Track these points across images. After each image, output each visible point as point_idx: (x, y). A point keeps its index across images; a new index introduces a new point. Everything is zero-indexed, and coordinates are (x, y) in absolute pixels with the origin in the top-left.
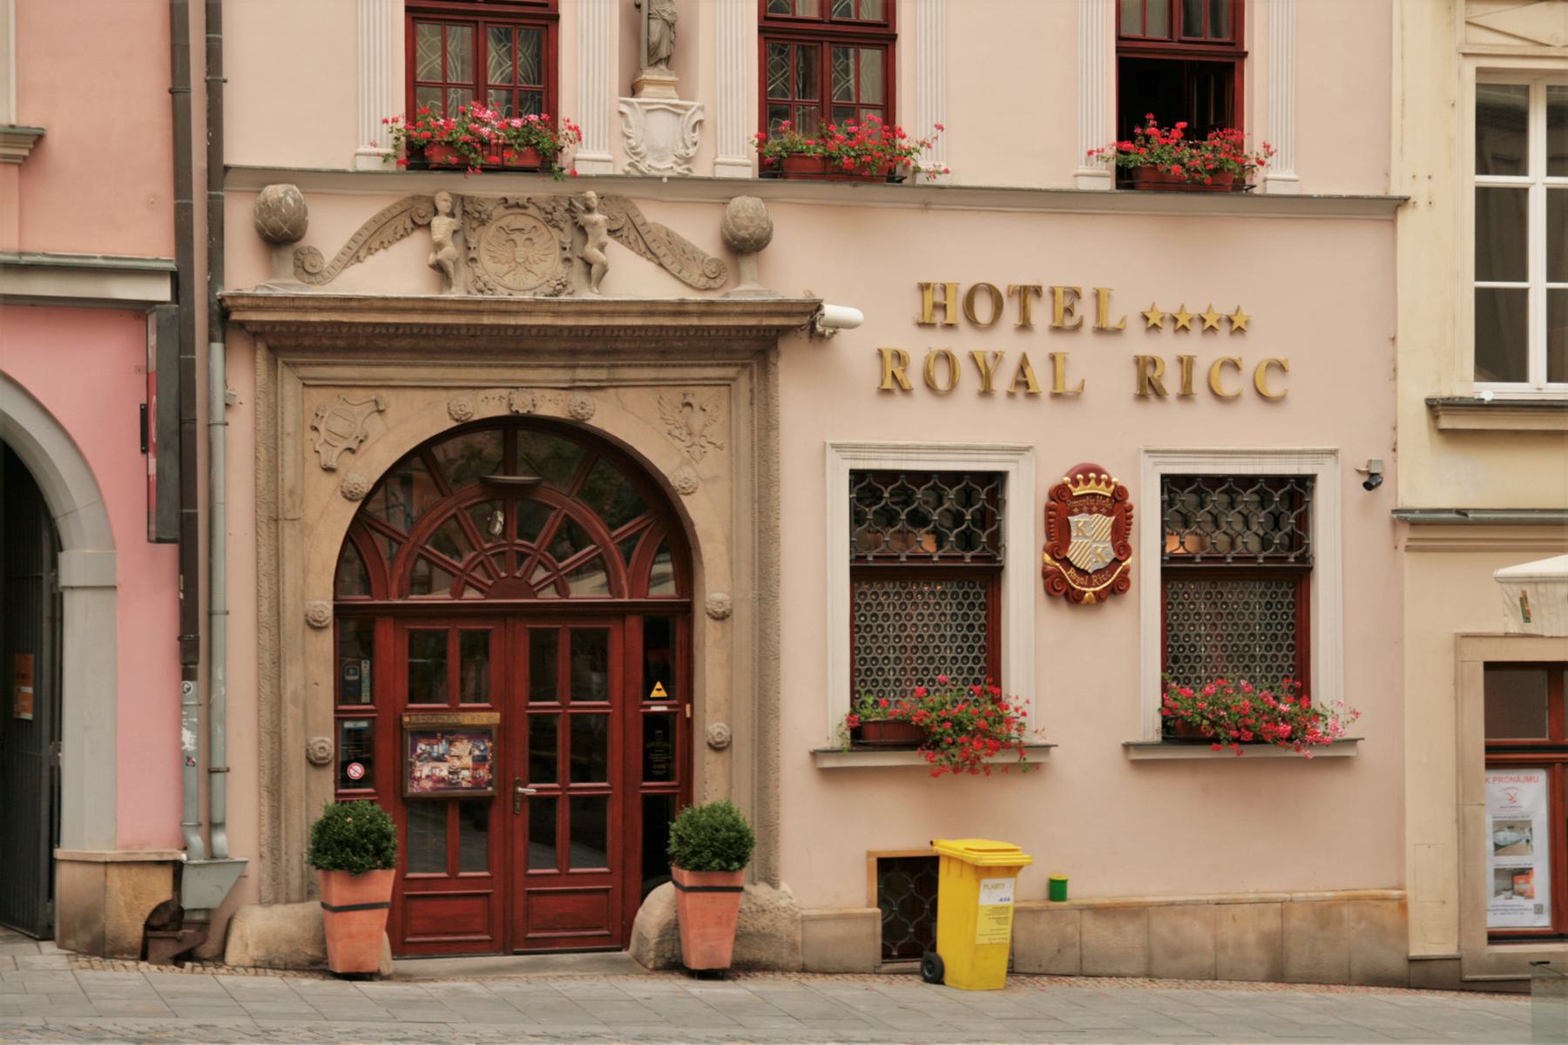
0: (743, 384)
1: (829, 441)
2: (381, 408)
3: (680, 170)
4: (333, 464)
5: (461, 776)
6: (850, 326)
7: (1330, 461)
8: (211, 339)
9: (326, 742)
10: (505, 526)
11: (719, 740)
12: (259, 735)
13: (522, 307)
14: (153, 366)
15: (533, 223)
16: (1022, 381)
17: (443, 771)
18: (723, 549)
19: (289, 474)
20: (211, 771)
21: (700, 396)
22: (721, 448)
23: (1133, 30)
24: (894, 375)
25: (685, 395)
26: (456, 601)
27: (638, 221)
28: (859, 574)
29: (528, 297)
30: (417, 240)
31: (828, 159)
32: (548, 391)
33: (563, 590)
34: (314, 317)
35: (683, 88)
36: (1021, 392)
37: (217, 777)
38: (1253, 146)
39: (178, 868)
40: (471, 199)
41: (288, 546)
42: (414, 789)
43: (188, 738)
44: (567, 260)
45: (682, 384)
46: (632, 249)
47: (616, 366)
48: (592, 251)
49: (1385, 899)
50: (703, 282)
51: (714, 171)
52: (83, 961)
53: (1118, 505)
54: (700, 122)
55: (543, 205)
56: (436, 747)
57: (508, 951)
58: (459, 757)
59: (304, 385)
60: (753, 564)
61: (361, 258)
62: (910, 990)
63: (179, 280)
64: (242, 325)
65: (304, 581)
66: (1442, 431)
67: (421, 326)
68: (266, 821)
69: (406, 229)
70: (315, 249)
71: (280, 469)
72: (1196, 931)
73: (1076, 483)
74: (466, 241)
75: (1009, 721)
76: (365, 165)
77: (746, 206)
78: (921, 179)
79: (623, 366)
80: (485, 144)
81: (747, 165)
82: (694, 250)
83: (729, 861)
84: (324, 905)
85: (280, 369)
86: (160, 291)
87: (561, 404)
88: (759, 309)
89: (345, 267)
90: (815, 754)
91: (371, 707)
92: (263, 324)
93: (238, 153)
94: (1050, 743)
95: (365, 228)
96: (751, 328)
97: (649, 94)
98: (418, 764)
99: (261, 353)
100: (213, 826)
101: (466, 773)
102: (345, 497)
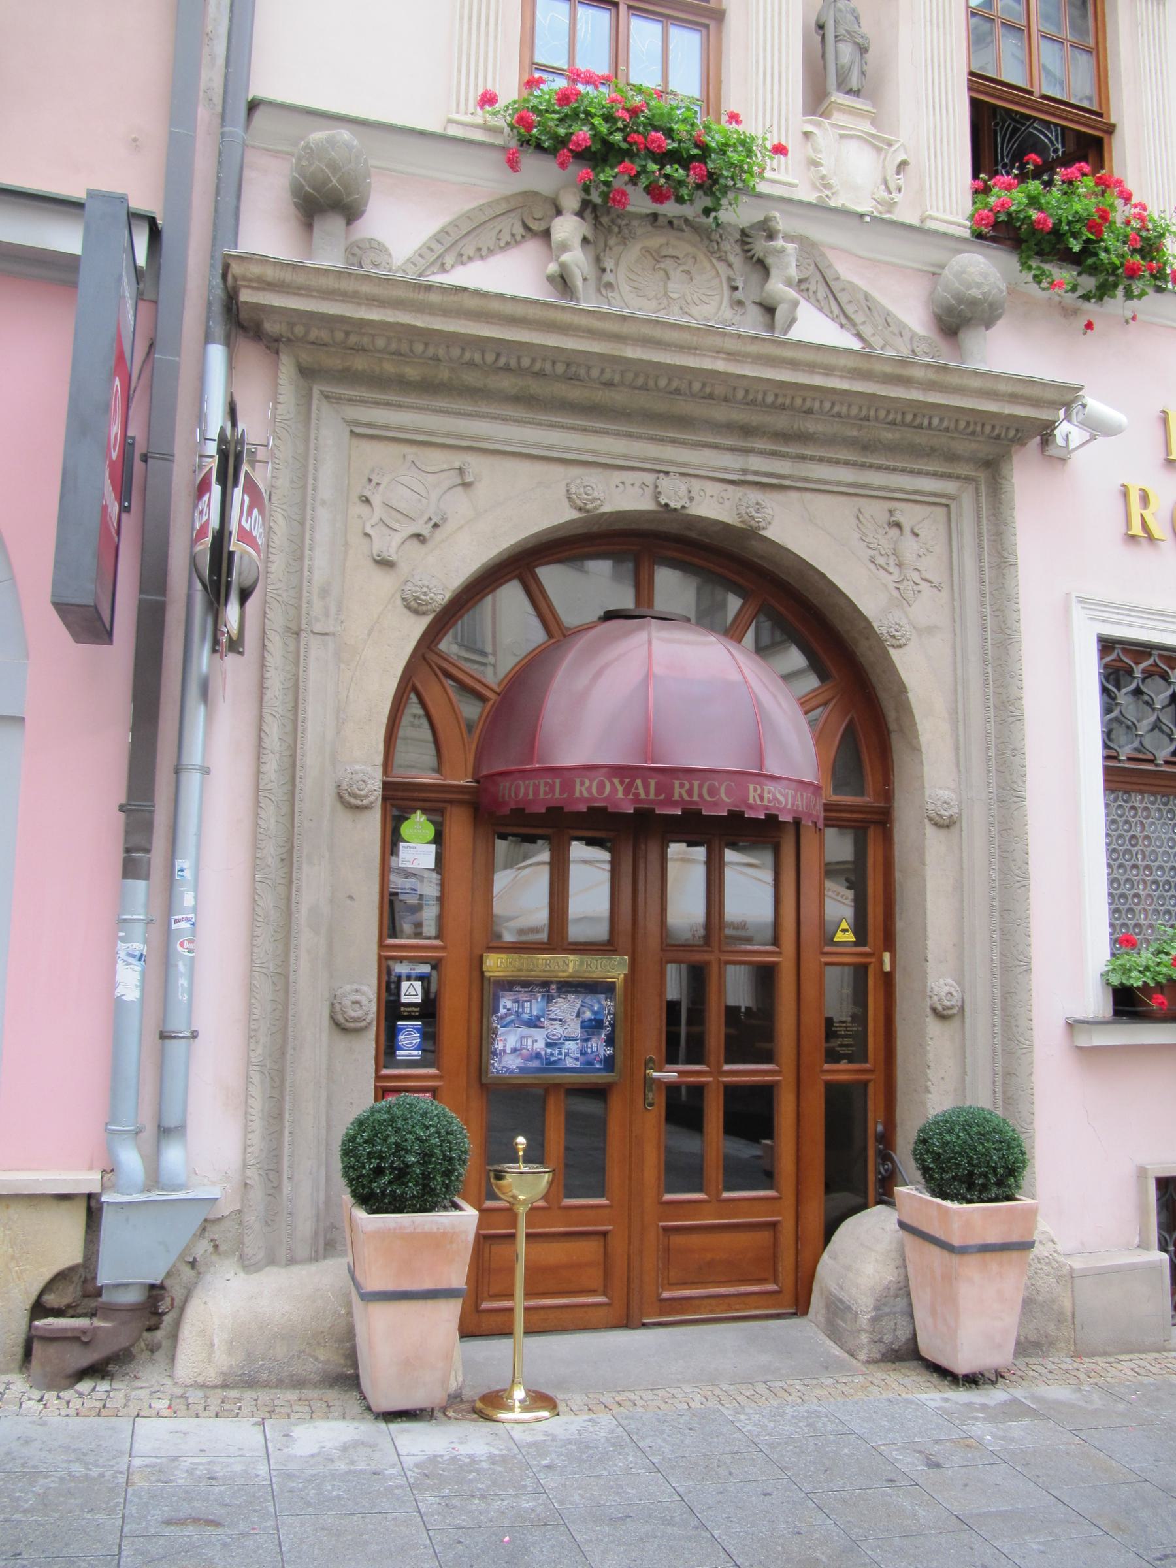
2: (469, 479)
4: (391, 554)
5: (563, 1051)
8: (208, 339)
9: (363, 994)
17: (537, 1041)
19: (320, 562)
20: (164, 1036)
21: (908, 515)
22: (938, 588)
25: (891, 512)
27: (829, 276)
32: (709, 484)
34: (374, 315)
41: (314, 676)
44: (740, 303)
45: (885, 495)
46: (821, 309)
54: (903, 164)
56: (527, 1005)
59: (352, 431)
61: (448, 266)
69: (513, 235)
70: (379, 243)
71: (307, 552)
79: (812, 458)
81: (964, 226)
85: (315, 402)
87: (727, 503)
90: (1073, 1026)
98: (501, 1030)
100: (166, 1132)
102: (408, 607)
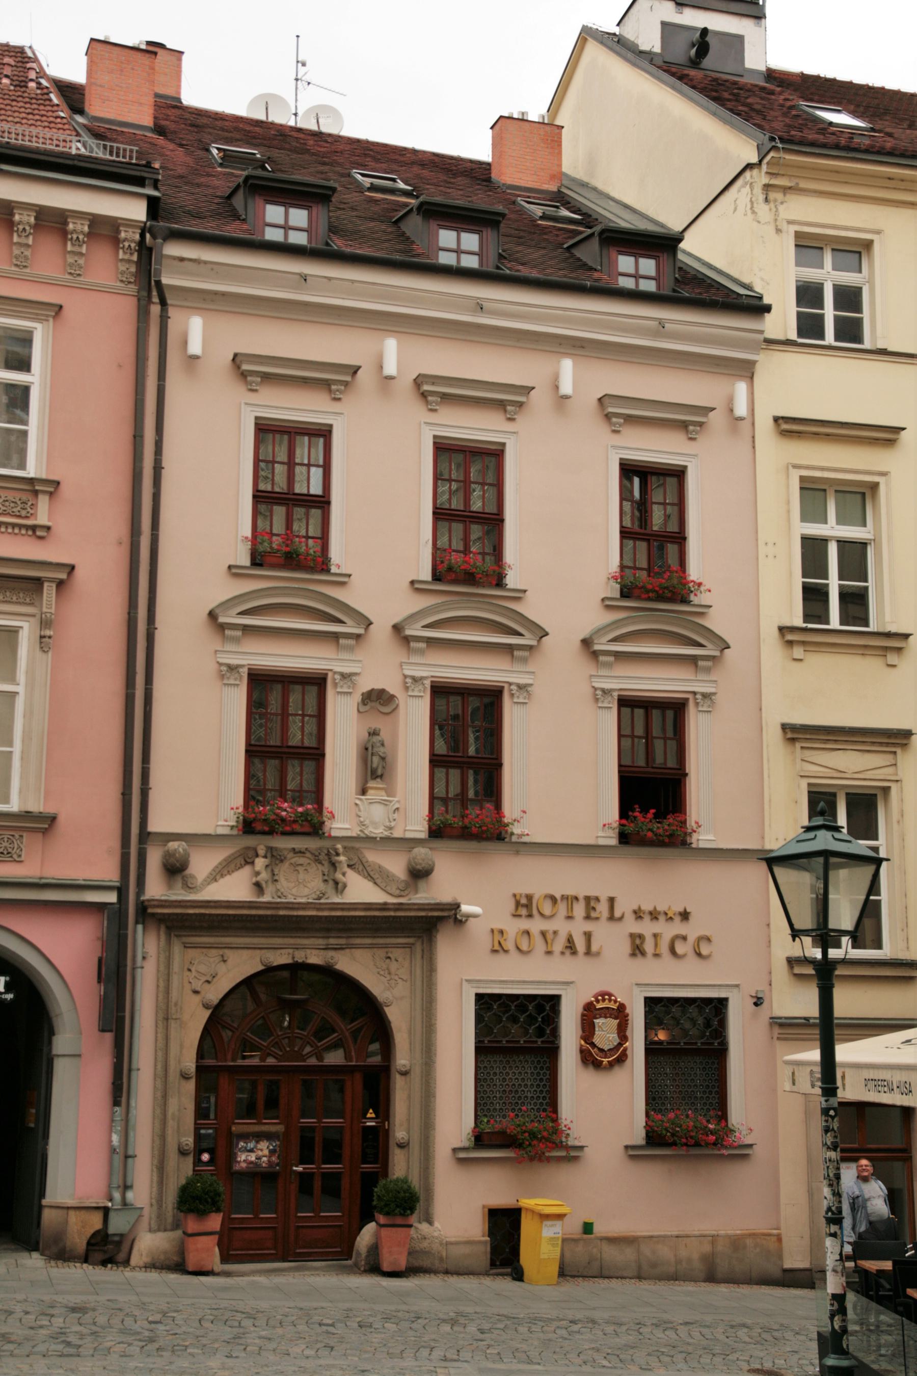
0: (418, 947)
1: (465, 978)
2: (225, 959)
3: (387, 833)
4: (198, 989)
6: (476, 916)
7: (735, 990)
8: (137, 922)
10: (290, 1022)
11: (402, 1141)
12: (153, 1136)
13: (300, 906)
14: (105, 939)
15: (308, 861)
16: (570, 946)
17: (252, 1157)
18: (406, 1036)
19: (174, 994)
21: (396, 953)
22: (406, 981)
23: (627, 761)
24: (500, 943)
25: (387, 953)
26: (263, 1064)
27: (364, 860)
28: (480, 1050)
29: (303, 900)
30: (246, 871)
31: (465, 828)
33: (320, 1058)
34: (191, 911)
35: (390, 792)
36: (568, 952)
37: (130, 1160)
38: (691, 822)
39: (106, 1211)
40: (276, 849)
41: (173, 1033)
42: (237, 1167)
43: (115, 1139)
44: (326, 881)
45: (385, 946)
47: (351, 937)
48: (339, 876)
49: (770, 1235)
50: (398, 892)
51: (404, 834)
52: (53, 1263)
53: (620, 1014)
54: (398, 809)
55: (314, 852)
57: (284, 1260)
58: (262, 1150)
60: (422, 1044)
62: (506, 1285)
63: (122, 891)
64: (153, 915)
65: (181, 1052)
66: (795, 975)
67: (247, 916)
68: (155, 1185)
72: (665, 1252)
73: (598, 1001)
74: (272, 871)
75: (562, 1131)
76: (221, 831)
77: (421, 852)
78: (514, 839)
79: (354, 937)
80: (283, 820)
81: (421, 831)
82: (394, 875)
83: (405, 1209)
84: (184, 1233)
85: (172, 938)
86: (111, 898)
88: (426, 907)
89: (209, 884)
90: (455, 1150)
91: (214, 1122)
92: (164, 914)
93: (154, 826)
94: (584, 1145)
95: (220, 864)
96: (422, 917)
97: (371, 795)
98: (239, 1153)
99: (163, 929)
100: (126, 1187)
101: (265, 1159)
